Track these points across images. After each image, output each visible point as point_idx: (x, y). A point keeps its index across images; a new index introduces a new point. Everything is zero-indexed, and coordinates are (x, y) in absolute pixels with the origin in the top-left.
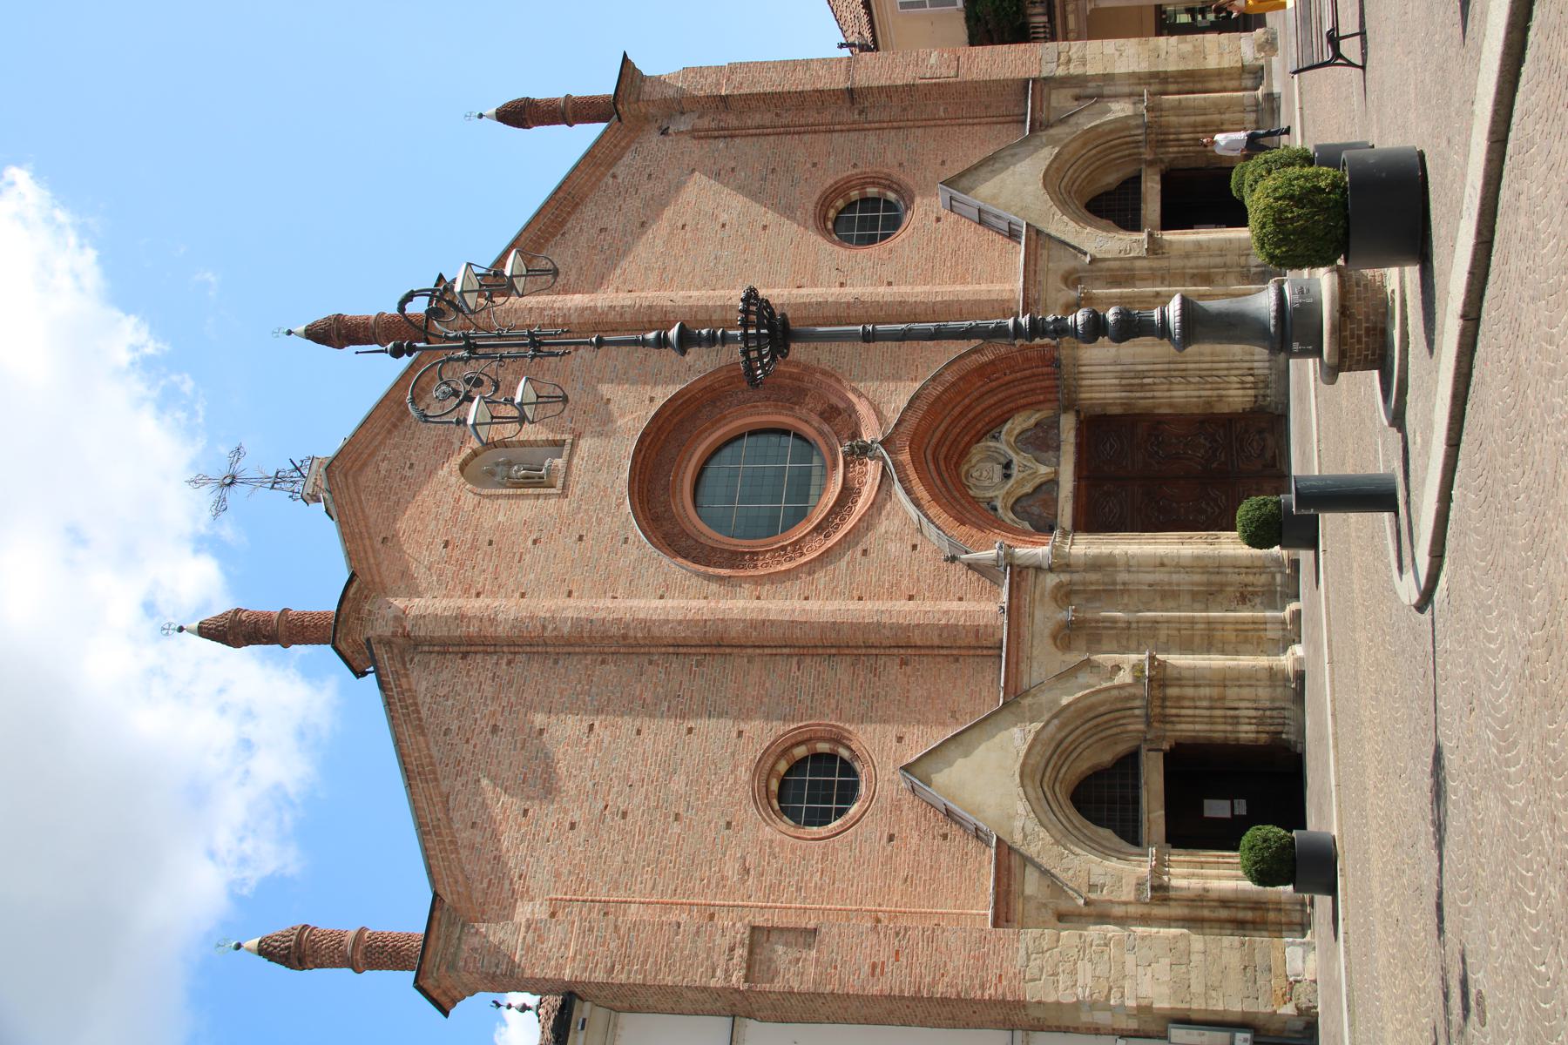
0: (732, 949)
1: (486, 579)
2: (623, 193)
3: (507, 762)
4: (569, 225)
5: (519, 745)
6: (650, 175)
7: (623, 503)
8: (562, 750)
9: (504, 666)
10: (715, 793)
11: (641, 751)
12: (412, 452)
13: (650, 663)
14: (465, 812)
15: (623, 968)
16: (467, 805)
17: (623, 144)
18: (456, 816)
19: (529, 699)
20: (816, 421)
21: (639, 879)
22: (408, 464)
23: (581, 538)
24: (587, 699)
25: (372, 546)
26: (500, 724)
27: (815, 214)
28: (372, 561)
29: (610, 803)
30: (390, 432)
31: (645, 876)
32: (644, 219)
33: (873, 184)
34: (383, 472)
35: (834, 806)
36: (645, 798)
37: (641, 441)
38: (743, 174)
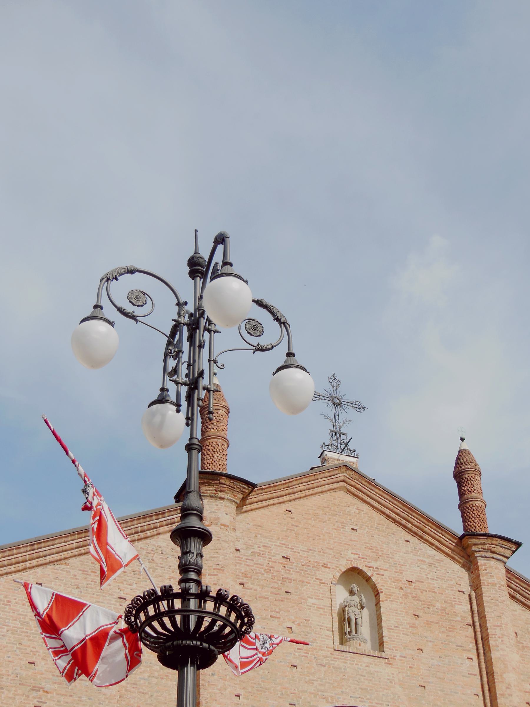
1: (255, 590)
12: (367, 530)
16: (57, 578)
24: (146, 675)
29: (49, 695)
34: (348, 509)
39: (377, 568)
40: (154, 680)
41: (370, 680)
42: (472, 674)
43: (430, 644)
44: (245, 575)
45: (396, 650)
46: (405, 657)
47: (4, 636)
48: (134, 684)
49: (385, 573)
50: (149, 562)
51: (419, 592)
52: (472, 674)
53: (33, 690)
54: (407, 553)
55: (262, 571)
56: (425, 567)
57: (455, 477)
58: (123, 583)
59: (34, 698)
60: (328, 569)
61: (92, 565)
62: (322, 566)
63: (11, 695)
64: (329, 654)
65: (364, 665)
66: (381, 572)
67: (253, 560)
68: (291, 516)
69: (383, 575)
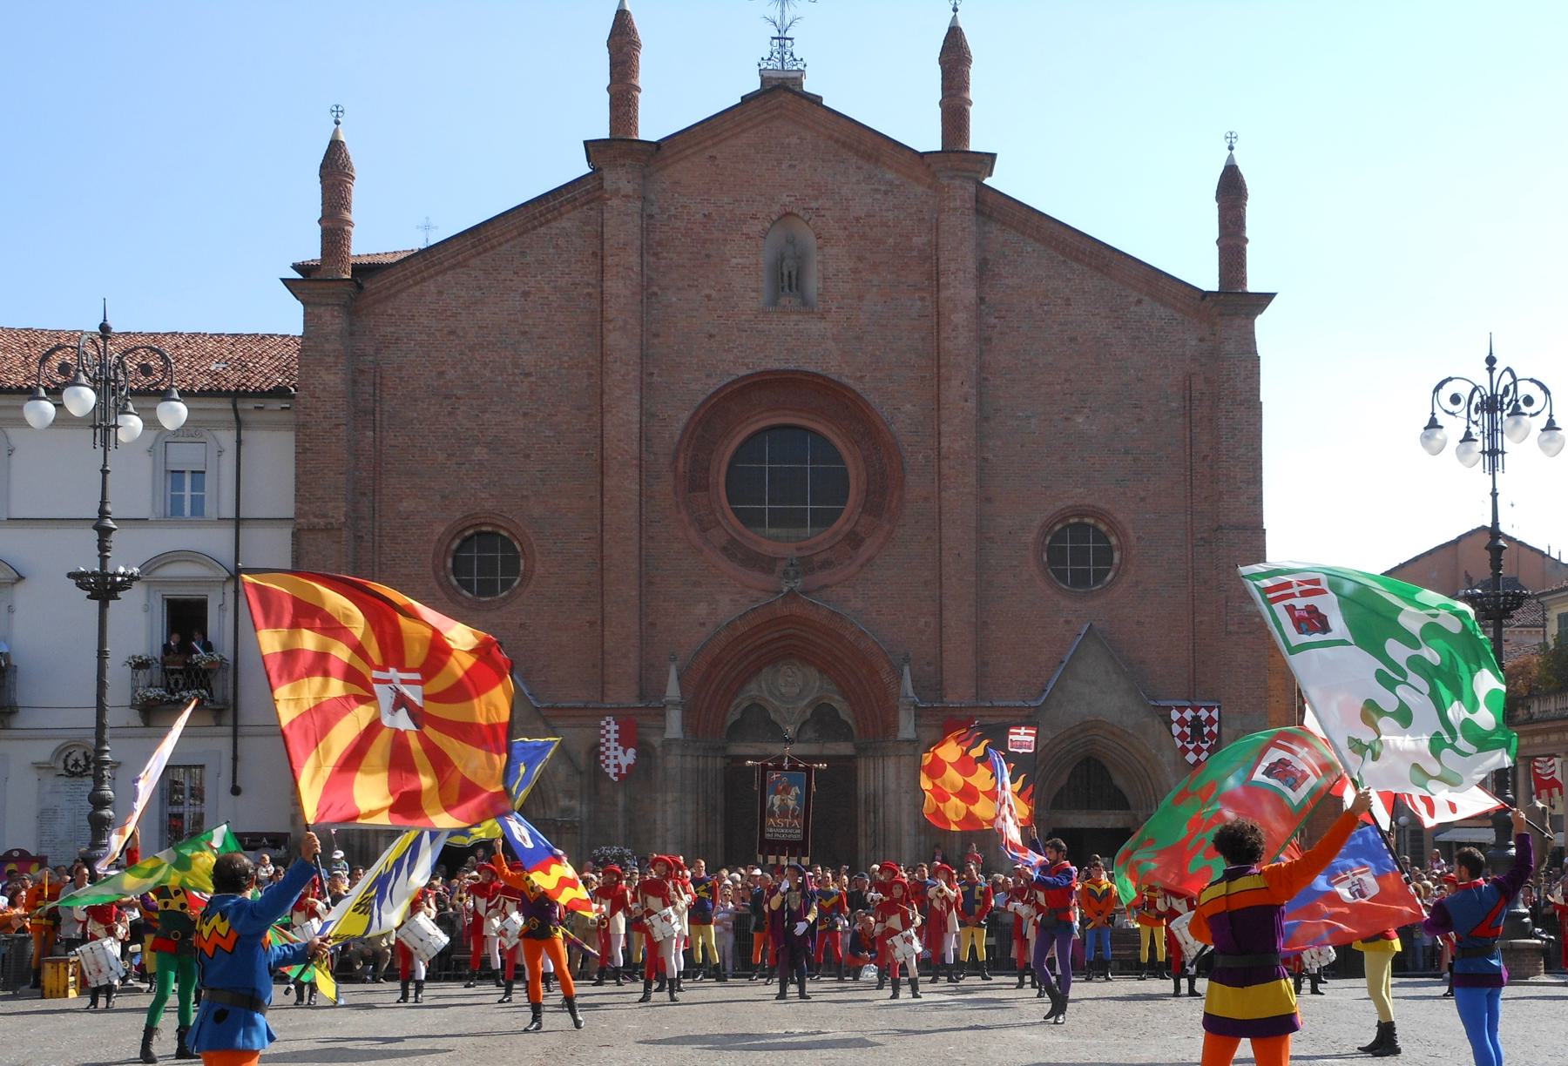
0: (324, 516)
2: (1116, 314)
3: (497, 310)
4: (1076, 266)
5: (512, 317)
6: (1138, 338)
7: (748, 368)
8: (507, 353)
9: (586, 291)
10: (473, 484)
11: (509, 418)
13: (590, 415)
14: (452, 282)
15: (307, 436)
16: (456, 283)
17: (1179, 305)
18: (449, 276)
19: (556, 318)
20: (847, 528)
21: (398, 434)
22: (794, 163)
23: (711, 336)
24: (555, 367)
25: (706, 148)
26: (532, 297)
27: (1081, 506)
28: (689, 152)
29: (462, 401)
30: (831, 137)
31: (400, 438)
32: (1081, 341)
33: (1121, 559)
35: (475, 578)
36: (467, 429)
37: (814, 375)
38: (1135, 431)
39: (818, 209)
40: (564, 372)
41: (798, 339)
42: (923, 316)
43: (875, 289)
44: (659, 243)
45: (832, 301)
46: (843, 308)
47: (412, 351)
48: (544, 378)
49: (828, 213)
50: (554, 248)
51: (867, 229)
52: (923, 316)
53: (445, 398)
54: (858, 182)
55: (679, 236)
56: (878, 196)
57: (942, 61)
58: (527, 277)
59: (448, 405)
60: (756, 221)
61: (493, 262)
62: (751, 218)
63: (425, 406)
64: (752, 317)
65: (792, 324)
66: (823, 212)
67: (669, 225)
68: (716, 163)
69: (824, 216)
